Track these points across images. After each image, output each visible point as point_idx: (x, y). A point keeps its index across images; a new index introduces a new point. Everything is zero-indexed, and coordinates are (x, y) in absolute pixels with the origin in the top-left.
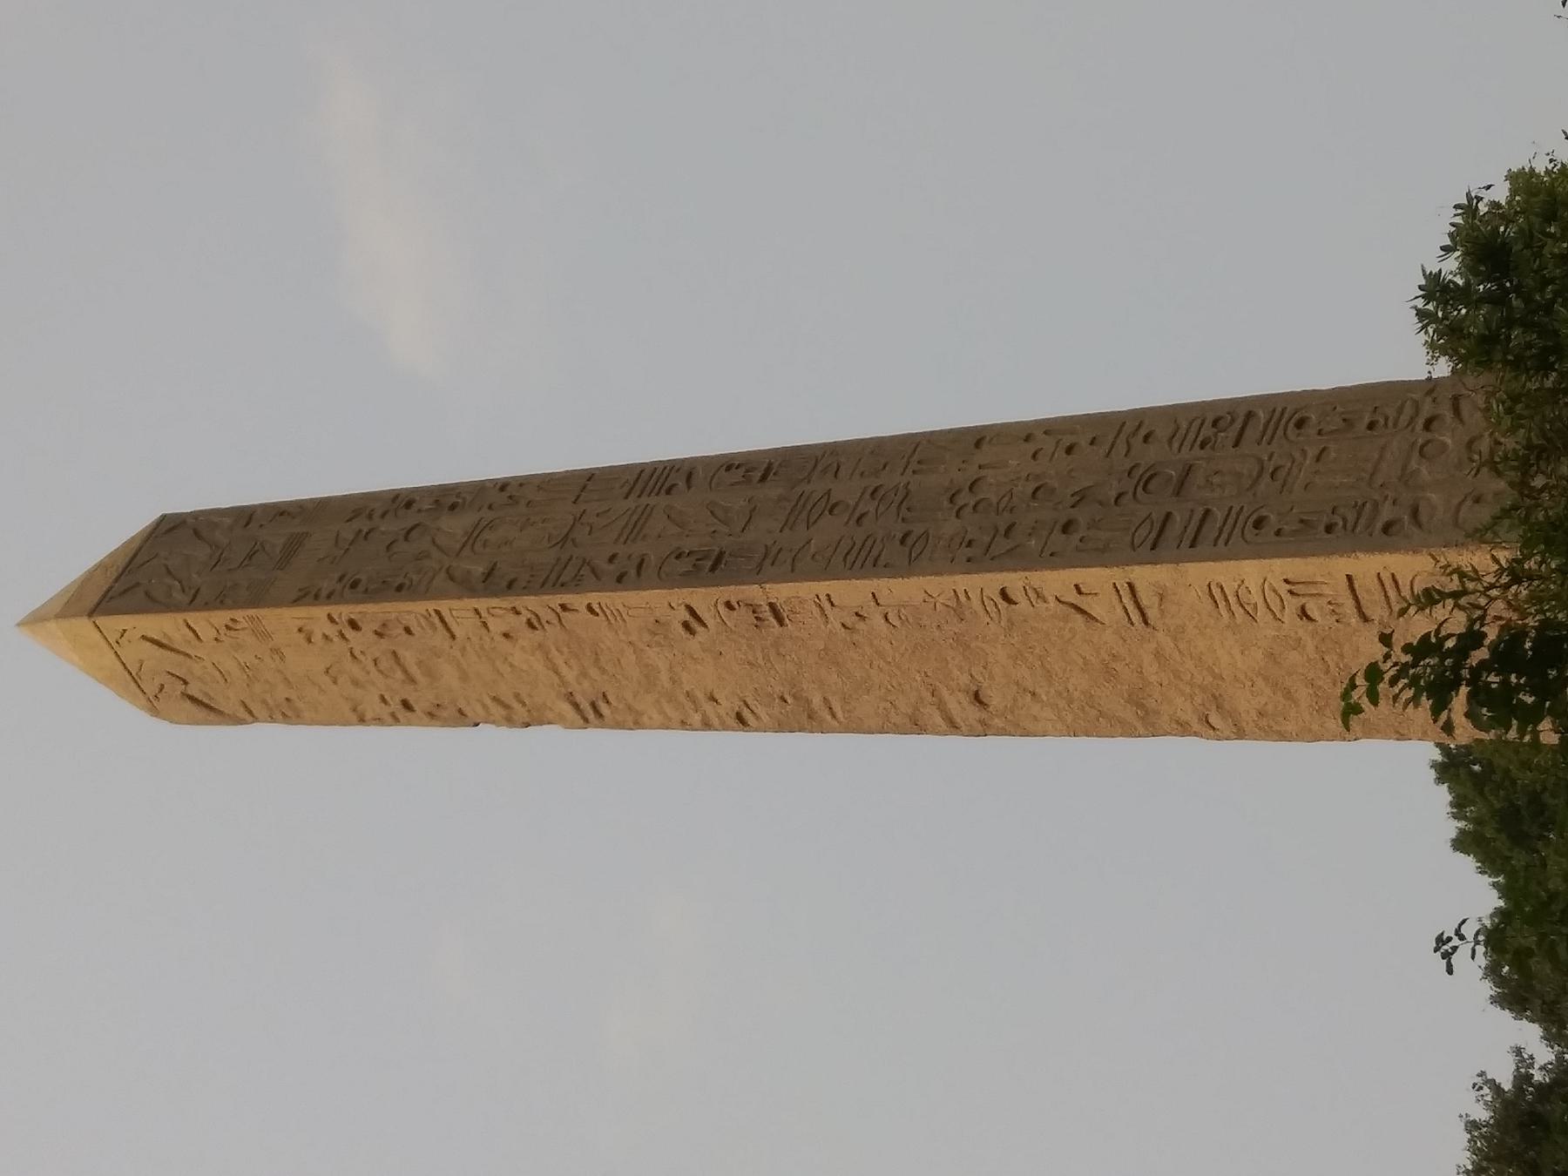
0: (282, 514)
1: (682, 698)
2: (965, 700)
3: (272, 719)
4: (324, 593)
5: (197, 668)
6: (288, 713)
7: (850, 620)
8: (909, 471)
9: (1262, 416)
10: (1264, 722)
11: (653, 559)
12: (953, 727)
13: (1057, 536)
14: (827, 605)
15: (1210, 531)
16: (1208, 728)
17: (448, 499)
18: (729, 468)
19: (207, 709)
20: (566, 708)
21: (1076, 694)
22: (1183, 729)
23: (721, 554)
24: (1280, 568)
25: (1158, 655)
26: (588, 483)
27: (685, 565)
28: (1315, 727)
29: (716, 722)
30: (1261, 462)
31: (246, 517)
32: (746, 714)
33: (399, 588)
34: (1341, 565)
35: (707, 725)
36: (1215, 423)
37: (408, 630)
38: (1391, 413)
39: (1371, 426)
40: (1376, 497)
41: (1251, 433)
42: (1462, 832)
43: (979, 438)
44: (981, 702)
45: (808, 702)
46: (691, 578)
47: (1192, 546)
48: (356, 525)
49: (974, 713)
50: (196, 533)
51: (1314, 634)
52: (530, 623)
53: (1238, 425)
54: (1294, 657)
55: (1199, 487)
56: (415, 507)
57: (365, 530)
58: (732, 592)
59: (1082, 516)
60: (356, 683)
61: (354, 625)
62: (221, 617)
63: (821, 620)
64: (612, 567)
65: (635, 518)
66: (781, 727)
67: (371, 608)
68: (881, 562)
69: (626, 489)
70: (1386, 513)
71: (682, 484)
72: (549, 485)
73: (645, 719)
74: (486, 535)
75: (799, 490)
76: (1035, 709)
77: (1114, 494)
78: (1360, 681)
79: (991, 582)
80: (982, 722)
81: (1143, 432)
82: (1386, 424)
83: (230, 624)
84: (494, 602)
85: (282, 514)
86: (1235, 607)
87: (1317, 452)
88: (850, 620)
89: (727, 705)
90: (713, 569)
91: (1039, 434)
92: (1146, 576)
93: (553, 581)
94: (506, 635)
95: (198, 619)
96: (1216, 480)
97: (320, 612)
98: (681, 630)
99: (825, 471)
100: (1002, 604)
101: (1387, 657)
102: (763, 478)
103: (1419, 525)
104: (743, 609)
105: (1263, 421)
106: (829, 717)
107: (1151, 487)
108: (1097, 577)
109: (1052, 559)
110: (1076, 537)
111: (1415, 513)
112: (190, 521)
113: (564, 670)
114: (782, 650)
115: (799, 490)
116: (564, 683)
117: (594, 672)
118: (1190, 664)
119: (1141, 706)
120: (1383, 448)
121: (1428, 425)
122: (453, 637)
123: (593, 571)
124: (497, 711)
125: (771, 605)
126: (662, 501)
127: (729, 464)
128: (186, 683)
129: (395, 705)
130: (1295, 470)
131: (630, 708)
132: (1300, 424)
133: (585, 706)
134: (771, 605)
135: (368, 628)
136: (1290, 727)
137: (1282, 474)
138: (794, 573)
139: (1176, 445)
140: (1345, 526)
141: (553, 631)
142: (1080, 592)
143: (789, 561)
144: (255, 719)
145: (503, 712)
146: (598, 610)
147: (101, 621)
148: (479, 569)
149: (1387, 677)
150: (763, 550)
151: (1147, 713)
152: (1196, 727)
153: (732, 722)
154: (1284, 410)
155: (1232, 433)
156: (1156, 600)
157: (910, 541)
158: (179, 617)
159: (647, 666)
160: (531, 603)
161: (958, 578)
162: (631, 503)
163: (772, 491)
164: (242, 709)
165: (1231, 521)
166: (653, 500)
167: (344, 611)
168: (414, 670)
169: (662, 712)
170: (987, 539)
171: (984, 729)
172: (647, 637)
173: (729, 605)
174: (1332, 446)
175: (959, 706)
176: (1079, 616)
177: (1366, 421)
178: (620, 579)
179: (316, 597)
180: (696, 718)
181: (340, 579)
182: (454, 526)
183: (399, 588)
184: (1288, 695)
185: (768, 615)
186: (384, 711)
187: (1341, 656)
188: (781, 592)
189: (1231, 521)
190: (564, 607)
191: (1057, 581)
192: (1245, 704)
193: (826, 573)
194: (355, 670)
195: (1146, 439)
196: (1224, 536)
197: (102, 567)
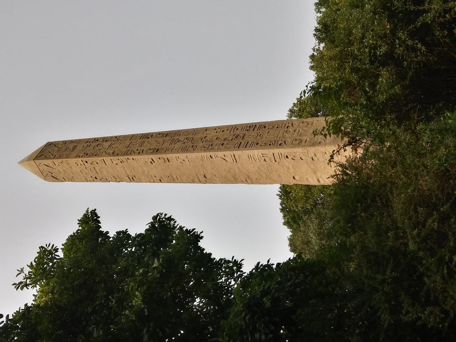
0: (72, 142)
1: (150, 176)
2: (203, 176)
3: (69, 181)
4: (81, 156)
5: (54, 170)
6: (72, 179)
7: (182, 161)
9: (258, 126)
12: (200, 182)
13: (221, 146)
15: (248, 145)
16: (247, 182)
17: (105, 139)
18: (159, 134)
19: (56, 179)
20: (127, 178)
22: (242, 182)
23: (158, 149)
25: (238, 168)
27: (151, 151)
28: (266, 182)
30: (257, 133)
31: (65, 142)
32: (161, 180)
35: (154, 182)
36: (249, 127)
37: (97, 163)
38: (281, 126)
39: (277, 127)
40: (278, 139)
41: (256, 129)
43: (206, 129)
44: (205, 177)
45: (173, 177)
46: (152, 153)
47: (245, 148)
48: (87, 144)
49: (204, 179)
50: (55, 145)
52: (121, 162)
53: (253, 127)
55: (246, 138)
56: (99, 141)
57: (89, 145)
58: (160, 156)
59: (225, 143)
60: (86, 174)
61: (86, 162)
62: (60, 160)
63: (177, 161)
64: (137, 151)
65: (142, 143)
66: (168, 182)
67: (90, 159)
68: (188, 150)
69: (140, 138)
70: (280, 142)
71: (151, 137)
73: (142, 181)
74: (113, 146)
75: (173, 138)
77: (231, 139)
78: (303, 92)
79: (209, 154)
80: (206, 181)
81: (236, 128)
82: (273, 144)
83: (62, 162)
84: (114, 157)
85: (72, 142)
86: (253, 159)
87: (268, 132)
88: (182, 161)
89: (158, 178)
90: (156, 152)
91: (217, 129)
92: (237, 153)
93: (126, 154)
94: (116, 164)
95: (56, 161)
96: (249, 136)
97: (80, 159)
98: (150, 163)
99: (177, 135)
100: (210, 158)
101: (307, 89)
102: (166, 136)
103: (286, 144)
104: (162, 159)
105: (258, 127)
107: (238, 137)
108: (228, 153)
109: (219, 150)
110: (224, 146)
111: (285, 142)
112: (54, 143)
113: (127, 171)
114: (169, 167)
115: (173, 138)
116: (127, 173)
117: (133, 172)
118: (244, 170)
119: (235, 178)
120: (279, 131)
121: (287, 128)
122: (106, 165)
123: (134, 152)
124: (114, 179)
125: (167, 158)
126: (147, 140)
127: (159, 134)
128: (52, 174)
129: (94, 178)
130: (264, 135)
131: (139, 178)
132: (265, 127)
133: (131, 178)
134: (167, 158)
135: (89, 162)
136: (262, 182)
137: (261, 136)
138: (172, 152)
139: (242, 131)
140: (273, 144)
141: (126, 163)
142: (224, 156)
143: (171, 150)
144: (66, 181)
145: (115, 179)
146: (134, 159)
147: (36, 161)
148: (111, 152)
149: (307, 92)
150: (166, 148)
151: (236, 179)
152: (245, 182)
153: (159, 181)
154: (262, 125)
156: (239, 157)
157: (194, 147)
158: (52, 160)
159: (143, 170)
160: (121, 158)
161: (202, 153)
162: (141, 140)
163: (167, 138)
164: (63, 179)
165: (252, 144)
166: (145, 140)
167: (85, 159)
168: (98, 171)
169: (146, 179)
171: (206, 182)
172: (143, 164)
173: (159, 158)
174: (270, 131)
176: (224, 160)
177: (276, 127)
178: (139, 154)
179: (79, 157)
180: (152, 180)
181: (84, 154)
182: (106, 144)
185: (166, 160)
187: (271, 168)
188: (169, 156)
189: (252, 144)
190: (128, 159)
191: (220, 154)
193: (178, 152)
194: (86, 171)
196: (251, 146)
197: (33, 153)
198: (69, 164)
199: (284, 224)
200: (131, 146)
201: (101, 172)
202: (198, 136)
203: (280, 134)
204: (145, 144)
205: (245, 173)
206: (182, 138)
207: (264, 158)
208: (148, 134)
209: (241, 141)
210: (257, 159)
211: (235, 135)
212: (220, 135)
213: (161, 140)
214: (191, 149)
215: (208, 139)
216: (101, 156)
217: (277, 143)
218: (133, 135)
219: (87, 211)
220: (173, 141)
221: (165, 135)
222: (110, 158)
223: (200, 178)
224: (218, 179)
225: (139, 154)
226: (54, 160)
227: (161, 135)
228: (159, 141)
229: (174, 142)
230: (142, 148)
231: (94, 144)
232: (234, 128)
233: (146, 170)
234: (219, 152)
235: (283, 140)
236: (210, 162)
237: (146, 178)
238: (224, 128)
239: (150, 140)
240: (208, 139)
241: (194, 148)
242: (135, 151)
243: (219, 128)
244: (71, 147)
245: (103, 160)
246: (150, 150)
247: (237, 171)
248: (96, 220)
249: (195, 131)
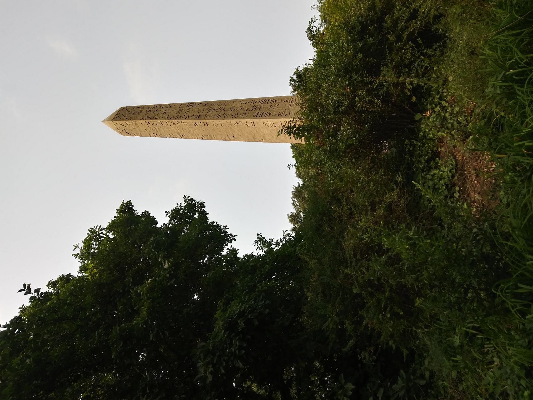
2: (232, 136)
3: (138, 136)
6: (140, 135)
7: (217, 125)
11: (190, 116)
12: (230, 140)
15: (263, 115)
16: (262, 141)
17: (162, 106)
19: (129, 134)
22: (259, 141)
24: (272, 120)
25: (256, 131)
26: (181, 105)
27: (195, 117)
31: (133, 108)
32: (203, 137)
33: (155, 118)
34: (280, 120)
35: (198, 139)
39: (284, 102)
41: (269, 102)
43: (234, 101)
46: (195, 118)
48: (149, 109)
49: (233, 138)
51: (276, 129)
54: (274, 132)
58: (201, 121)
59: (247, 112)
60: (149, 131)
61: (149, 123)
62: (130, 121)
67: (151, 121)
70: (286, 113)
72: (176, 105)
78: (280, 131)
79: (235, 121)
84: (169, 121)
88: (217, 125)
89: (201, 136)
92: (255, 121)
93: (177, 118)
95: (127, 122)
97: (144, 121)
100: (237, 124)
102: (205, 105)
108: (249, 121)
109: (243, 118)
110: (246, 115)
113: (178, 130)
116: (178, 132)
117: (182, 131)
118: (260, 133)
121: (291, 102)
126: (191, 108)
127: (200, 103)
132: (275, 101)
136: (273, 141)
137: (273, 108)
138: (209, 118)
141: (177, 125)
147: (113, 121)
148: (166, 116)
155: (267, 102)
158: (124, 121)
162: (187, 108)
163: (206, 107)
166: (190, 108)
167: (148, 121)
168: (158, 130)
171: (234, 140)
172: (189, 126)
174: (279, 104)
175: (231, 137)
180: (196, 138)
182: (163, 110)
183: (155, 118)
184: (273, 137)
185: (206, 124)
188: (207, 121)
191: (244, 121)
192: (267, 138)
193: (214, 119)
194: (149, 129)
198: (137, 124)
199: (293, 157)
200: (180, 112)
201: (160, 130)
202: (228, 107)
203: (286, 107)
204: (191, 111)
206: (216, 107)
208: (193, 103)
209: (259, 111)
211: (254, 107)
212: (244, 106)
213: (201, 108)
214: (223, 116)
215: (235, 109)
216: (159, 119)
217: (284, 114)
218: (182, 104)
219: (123, 203)
220: (210, 110)
221: (204, 105)
222: (166, 121)
223: (230, 137)
224: (242, 138)
226: (126, 121)
228: (200, 109)
230: (188, 114)
231: (154, 110)
232: (254, 101)
234: (243, 120)
235: (288, 111)
238: (246, 101)
239: (193, 108)
240: (235, 109)
241: (225, 116)
242: (183, 116)
243: (243, 100)
244: (138, 111)
247: (255, 133)
248: (131, 208)
249: (226, 103)
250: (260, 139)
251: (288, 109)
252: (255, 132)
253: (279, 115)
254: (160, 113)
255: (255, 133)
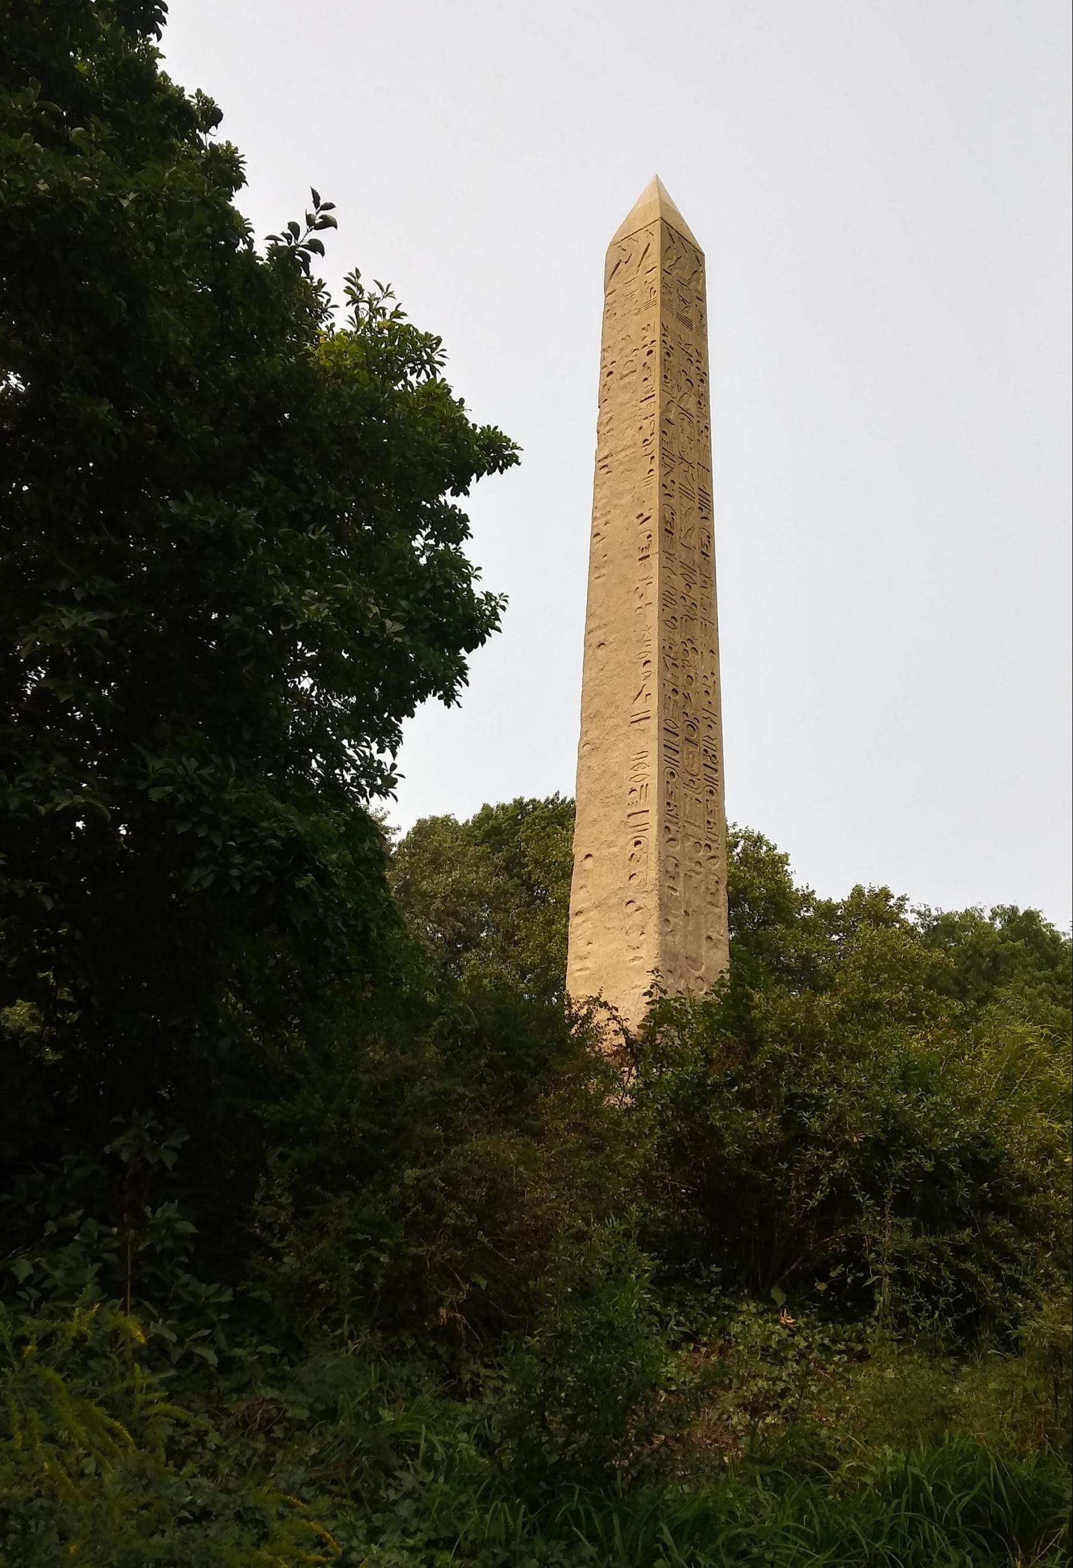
1: (608, 509)
2: (602, 639)
4: (665, 338)
5: (633, 269)
6: (609, 313)
7: (640, 591)
8: (703, 620)
9: (715, 776)
10: (585, 768)
11: (672, 501)
12: (589, 632)
13: (672, 687)
14: (647, 581)
15: (670, 753)
16: (583, 744)
17: (703, 401)
18: (708, 537)
19: (613, 271)
21: (601, 688)
22: (584, 733)
23: (672, 534)
24: (654, 783)
25: (618, 726)
26: (706, 469)
27: (668, 517)
29: (595, 523)
31: (701, 298)
32: (598, 538)
33: (665, 377)
34: (653, 809)
35: (594, 519)
36: (713, 755)
37: (646, 379)
38: (712, 831)
39: (709, 822)
40: (680, 824)
41: (709, 771)
42: (492, 810)
43: (714, 652)
45: (603, 567)
46: (663, 520)
47: (665, 746)
48: (695, 354)
49: (595, 642)
51: (623, 793)
52: (646, 440)
53: (712, 765)
54: (614, 784)
56: (700, 384)
59: (679, 698)
60: (622, 349)
61: (650, 352)
62: (657, 285)
63: (641, 578)
64: (669, 481)
68: (665, 608)
69: (702, 488)
70: (673, 828)
71: (703, 515)
72: (706, 450)
75: (697, 569)
76: (595, 669)
77: (687, 712)
79: (654, 657)
80: (590, 645)
81: (712, 724)
83: (653, 290)
84: (657, 424)
86: (637, 761)
88: (640, 591)
89: (603, 530)
90: (666, 530)
91: (714, 679)
92: (653, 724)
93: (665, 454)
94: (641, 428)
95: (656, 274)
96: (691, 756)
97: (657, 337)
98: (640, 513)
104: (648, 543)
106: (596, 576)
108: (653, 703)
109: (662, 685)
110: (670, 694)
111: (672, 840)
113: (624, 454)
115: (697, 569)
117: (622, 468)
118: (612, 739)
119: (595, 717)
121: (707, 845)
124: (606, 418)
125: (649, 556)
127: (710, 537)
129: (610, 368)
133: (606, 462)
134: (649, 556)
136: (583, 779)
137: (691, 784)
138: (663, 567)
139: (706, 739)
144: (606, 297)
145: (605, 421)
147: (658, 223)
148: (671, 417)
153: (595, 532)
155: (709, 763)
156: (642, 728)
158: (658, 264)
160: (656, 442)
161: (657, 642)
162: (697, 491)
163: (697, 557)
166: (697, 501)
167: (657, 349)
168: (626, 380)
169: (602, 498)
170: (672, 655)
171: (587, 646)
172: (637, 496)
173: (649, 536)
174: (702, 805)
175: (598, 637)
176: (637, 694)
178: (664, 485)
179: (664, 335)
180: (598, 515)
181: (671, 347)
182: (691, 404)
183: (665, 377)
184: (597, 780)
185: (645, 554)
186: (608, 362)
187: (613, 804)
188: (654, 561)
190: (653, 458)
191: (653, 685)
192: (594, 761)
194: (628, 350)
195: (709, 726)
196: (668, 759)
198: (647, 308)
199: (486, 807)
200: (684, 466)
201: (625, 387)
202: (698, 632)
203: (692, 827)
204: (686, 502)
205: (605, 742)
206: (695, 592)
207: (638, 788)
208: (710, 510)
209: (682, 736)
210: (637, 773)
211: (695, 722)
212: (699, 685)
213: (693, 541)
214: (669, 612)
218: (709, 471)
219: (515, 447)
220: (688, 571)
222: (657, 412)
223: (598, 633)
224: (593, 675)
225: (664, 485)
226: (658, 270)
227: (705, 540)
228: (691, 536)
229: (687, 572)
230: (677, 494)
232: (713, 720)
233: (623, 501)
234: (656, 682)
235: (679, 836)
236: (636, 660)
237: (604, 501)
238: (714, 693)
239: (696, 513)
241: (669, 622)
242: (671, 477)
243: (716, 683)
244: (689, 314)
245: (653, 395)
246: (672, 513)
247: (611, 722)
248: (496, 465)
249: (710, 625)
250: (592, 735)
251: (687, 836)
252: (616, 721)
253: (668, 804)
254: (681, 394)
255: (611, 722)
